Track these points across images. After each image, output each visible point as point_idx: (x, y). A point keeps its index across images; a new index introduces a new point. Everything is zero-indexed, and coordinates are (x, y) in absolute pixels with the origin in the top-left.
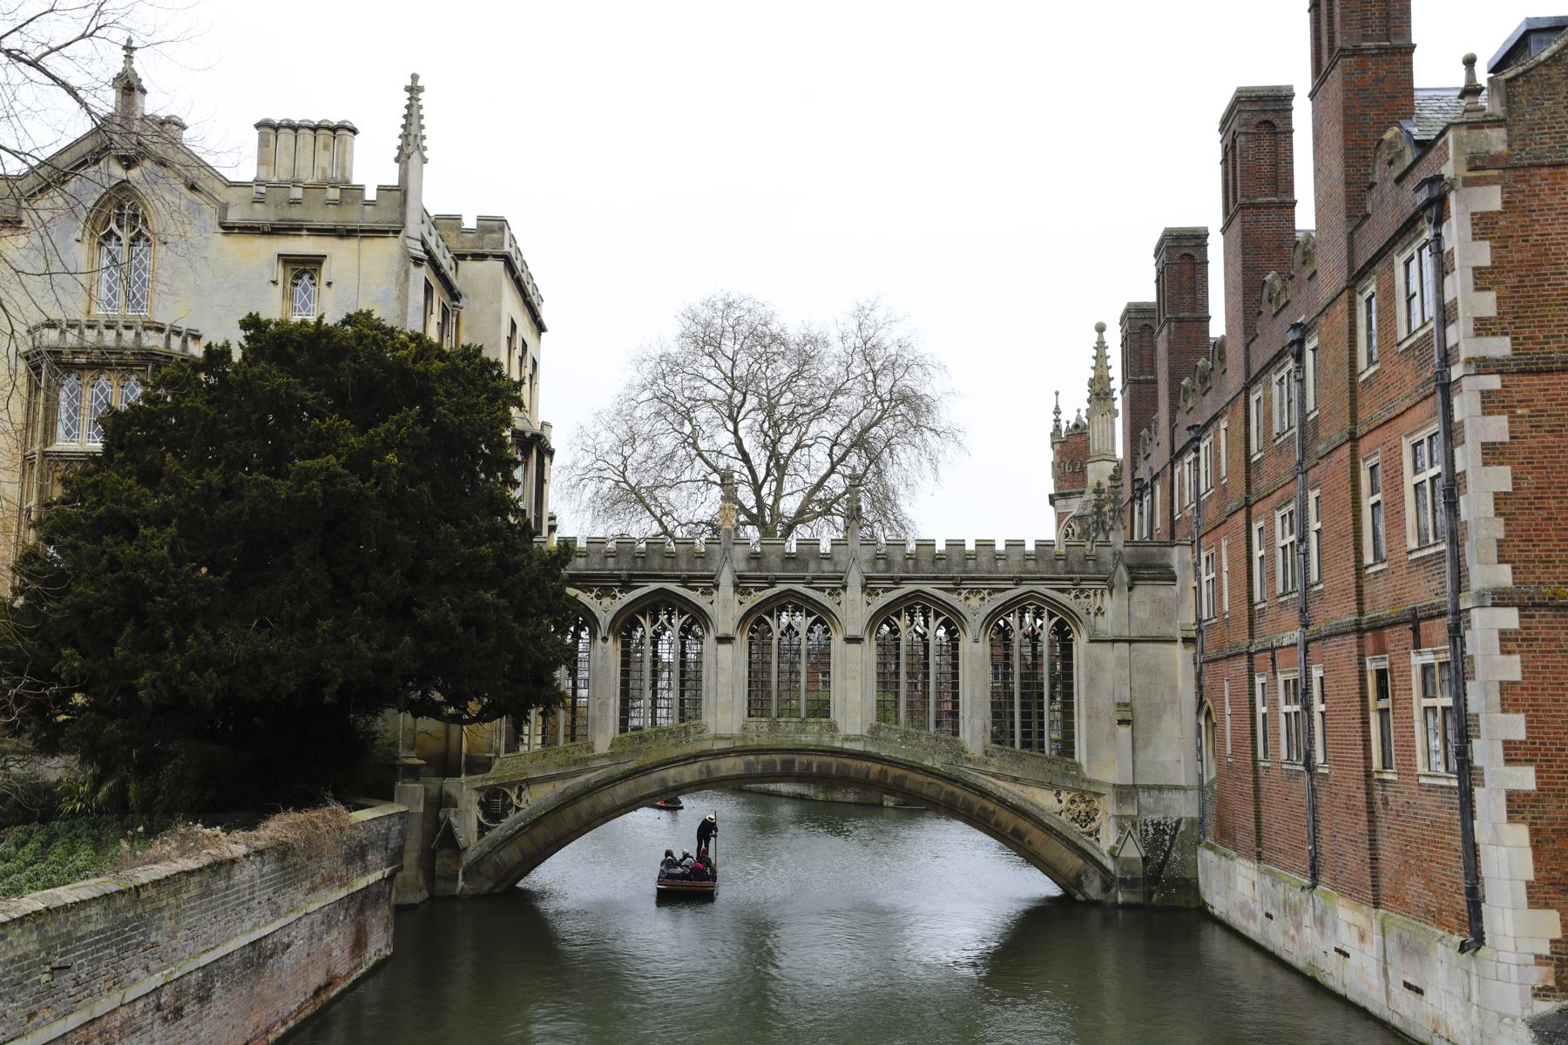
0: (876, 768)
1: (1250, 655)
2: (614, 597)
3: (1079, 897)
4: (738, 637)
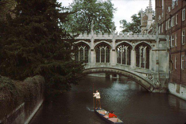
1: (181, 52)
3: (149, 90)
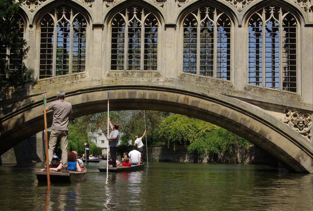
0: (182, 97)
2: (37, 4)
4: (105, 25)
